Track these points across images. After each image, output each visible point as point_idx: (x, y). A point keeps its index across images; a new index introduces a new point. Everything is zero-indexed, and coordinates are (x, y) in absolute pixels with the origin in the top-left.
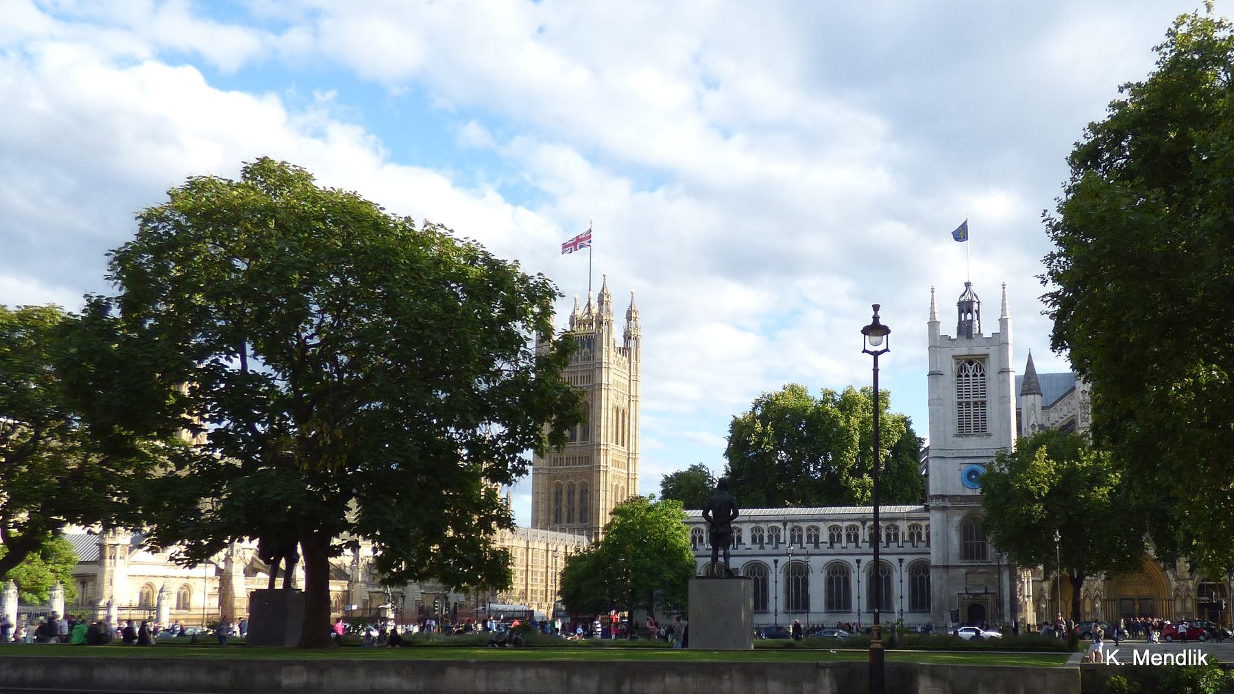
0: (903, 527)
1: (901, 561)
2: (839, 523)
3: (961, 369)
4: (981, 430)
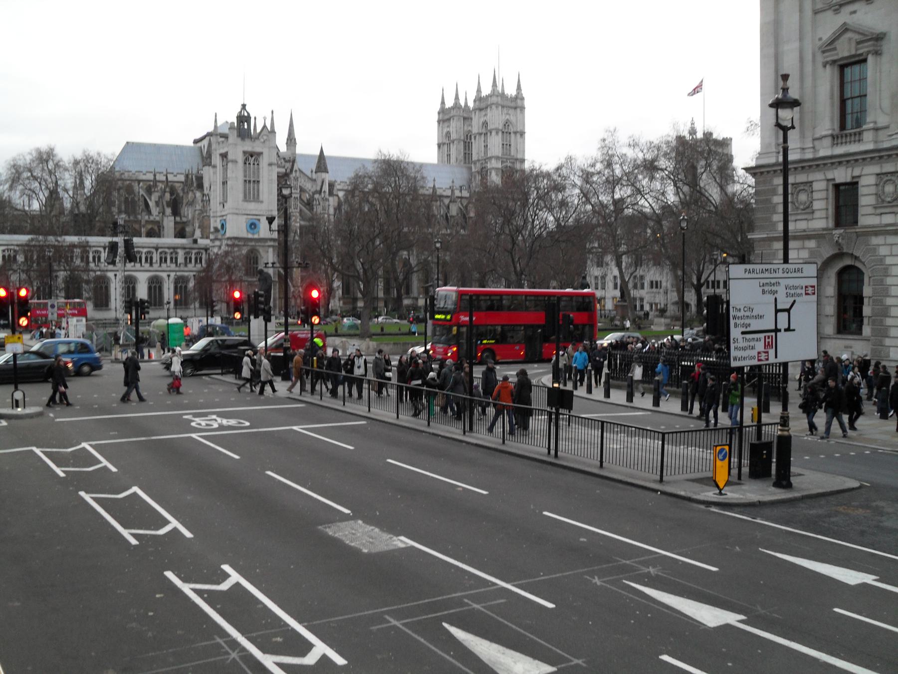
4: (256, 199)
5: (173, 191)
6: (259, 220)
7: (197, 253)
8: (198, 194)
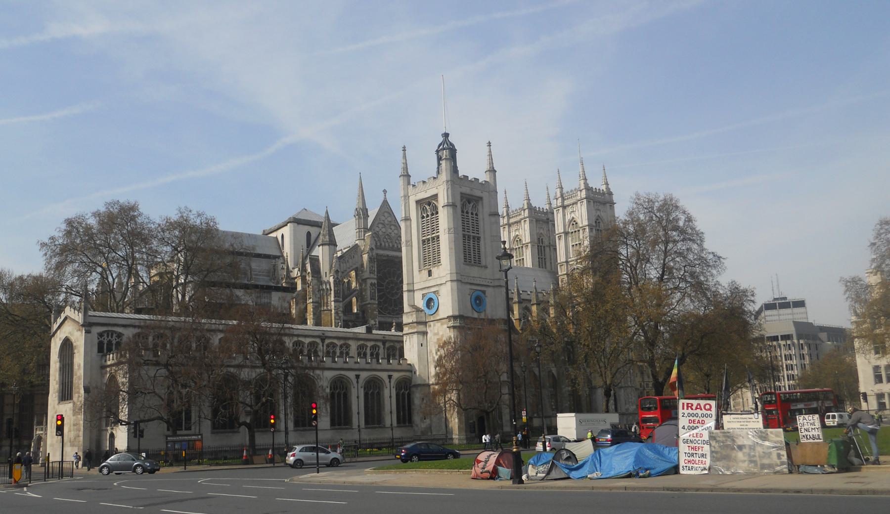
0: (354, 345)
1: (390, 377)
3: (463, 206)
6: (484, 292)
7: (373, 347)
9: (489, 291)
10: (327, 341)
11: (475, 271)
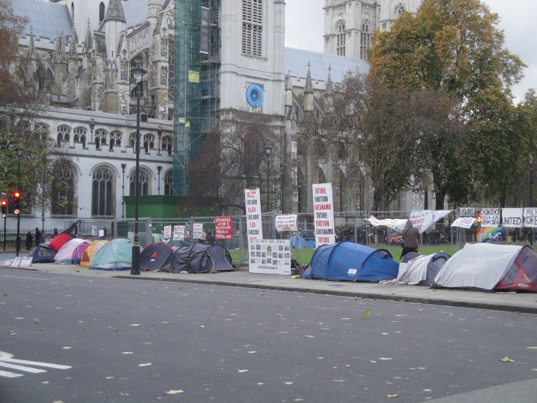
0: (126, 135)
2: (68, 124)
5: (38, 60)
6: (262, 86)
7: (148, 136)
8: (99, 61)
9: (268, 85)
10: (96, 127)
11: (253, 64)
